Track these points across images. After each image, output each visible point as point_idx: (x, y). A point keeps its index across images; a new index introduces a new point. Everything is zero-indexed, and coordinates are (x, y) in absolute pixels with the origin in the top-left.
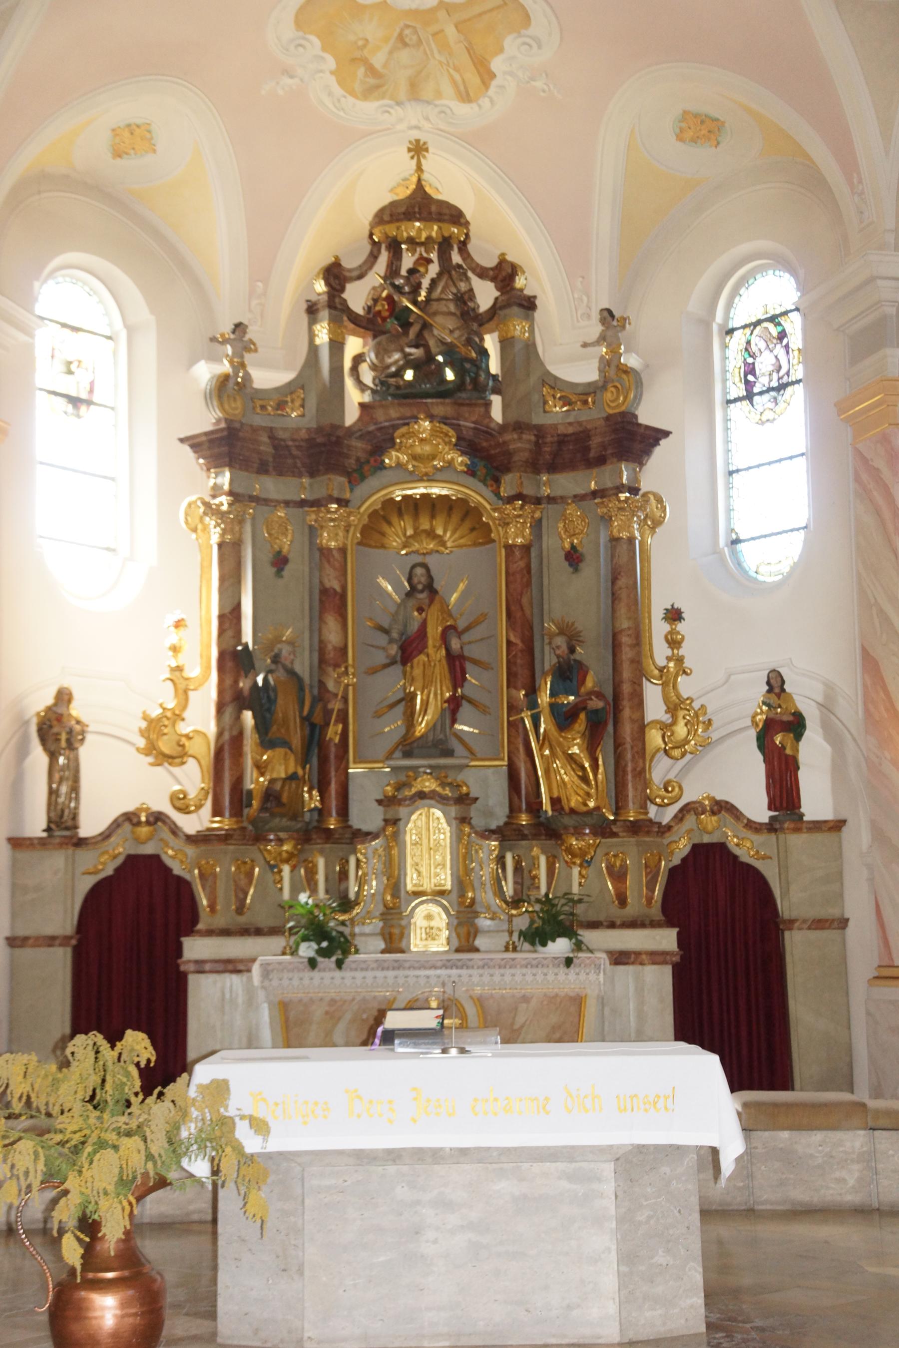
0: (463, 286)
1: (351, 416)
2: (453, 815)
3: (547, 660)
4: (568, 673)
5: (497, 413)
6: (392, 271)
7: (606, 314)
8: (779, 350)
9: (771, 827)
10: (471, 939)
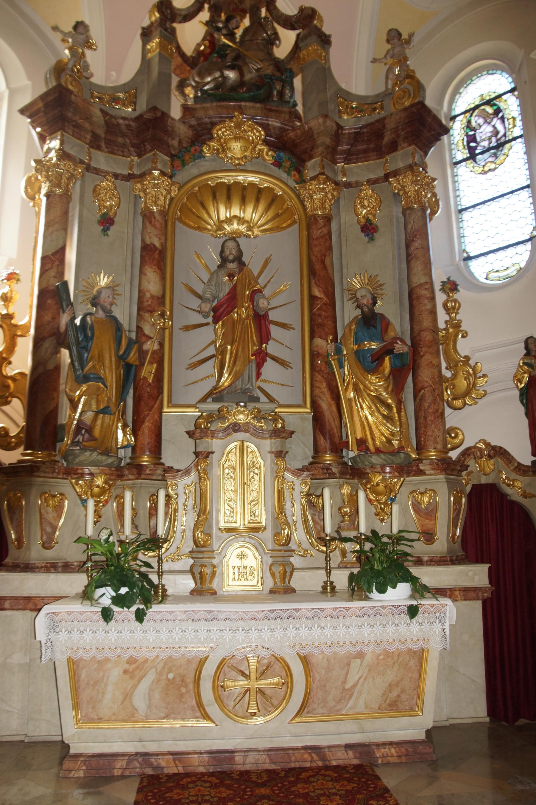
2: (268, 449)
3: (347, 314)
7: (394, 34)
10: (287, 580)
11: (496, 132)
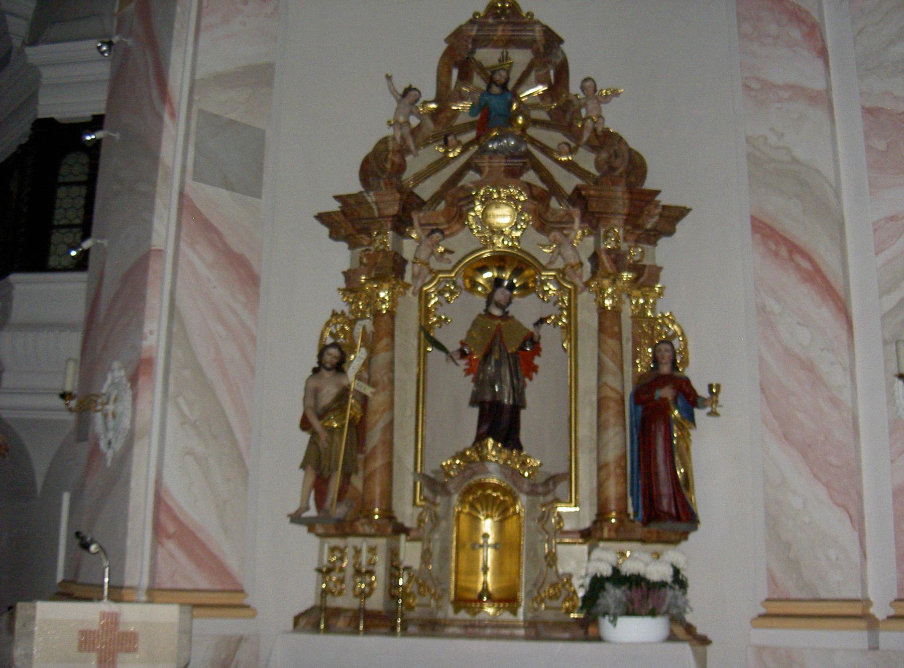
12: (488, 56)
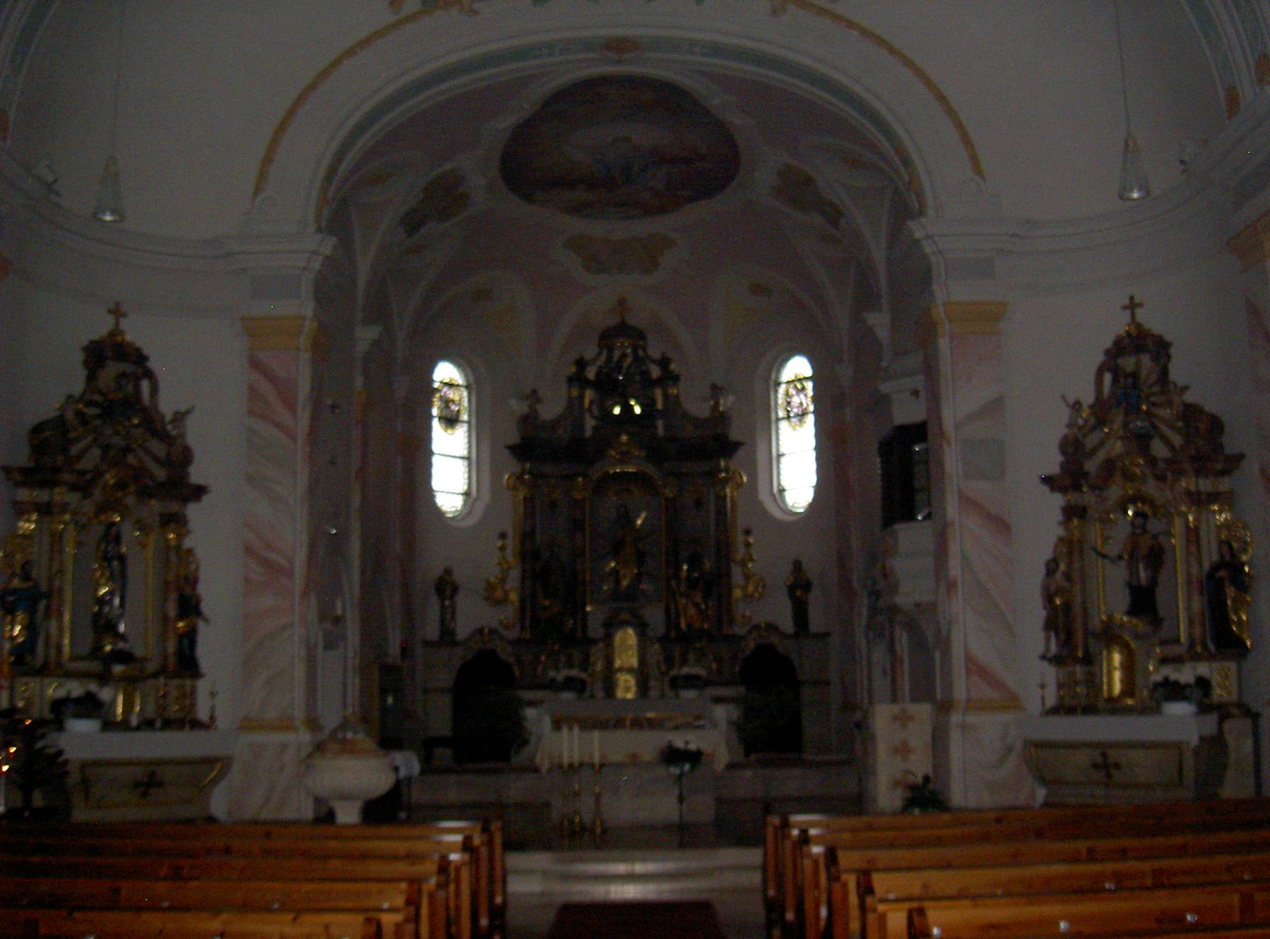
0: (644, 368)
1: (588, 432)
4: (695, 562)
5: (661, 431)
6: (609, 358)
8: (802, 396)
9: (796, 635)
11: (801, 404)
12: (1128, 363)
